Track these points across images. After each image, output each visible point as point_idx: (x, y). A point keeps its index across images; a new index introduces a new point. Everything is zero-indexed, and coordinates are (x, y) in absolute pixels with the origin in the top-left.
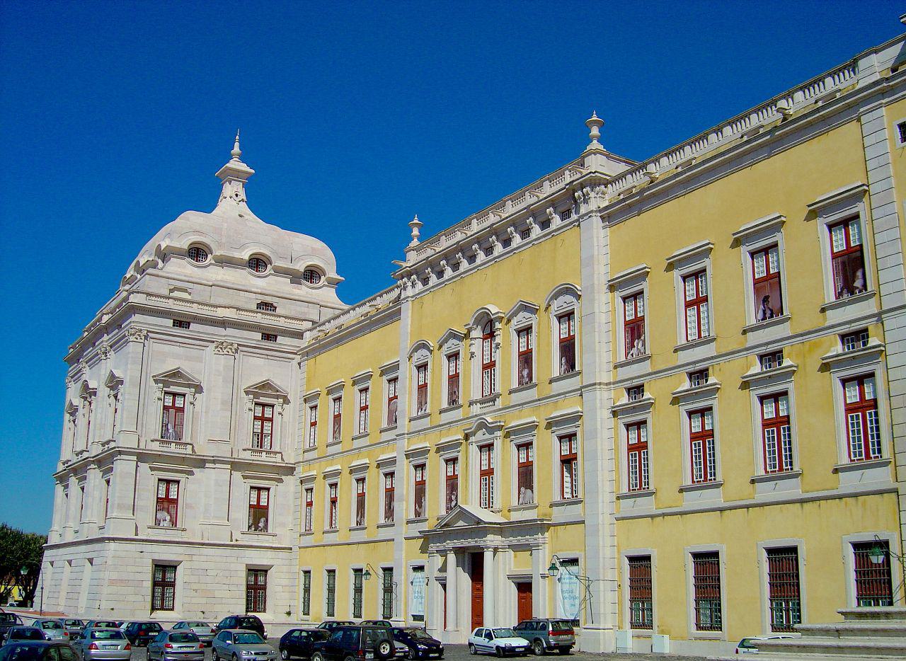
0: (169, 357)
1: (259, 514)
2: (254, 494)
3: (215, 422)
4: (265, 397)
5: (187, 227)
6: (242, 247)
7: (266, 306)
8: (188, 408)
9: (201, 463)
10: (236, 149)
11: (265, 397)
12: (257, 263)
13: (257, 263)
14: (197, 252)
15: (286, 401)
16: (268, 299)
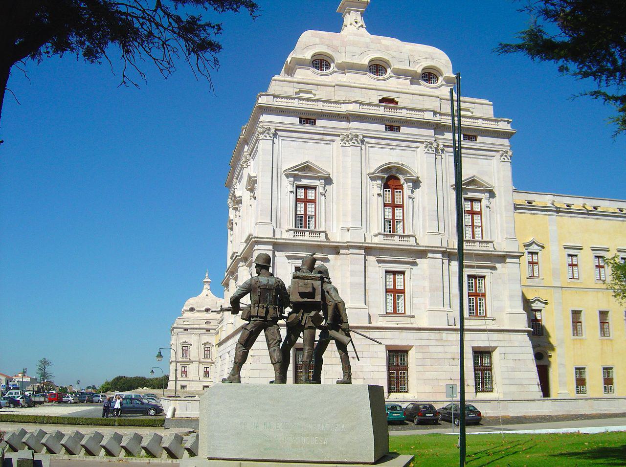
0: (184, 338)
1: (206, 374)
2: (205, 368)
3: (194, 353)
4: (207, 347)
5: (191, 302)
6: (203, 306)
7: (208, 323)
8: (189, 350)
9: (192, 362)
10: (207, 275)
11: (207, 347)
12: (207, 310)
13: (207, 310)
14: (192, 310)
15: (213, 346)
16: (208, 321)
